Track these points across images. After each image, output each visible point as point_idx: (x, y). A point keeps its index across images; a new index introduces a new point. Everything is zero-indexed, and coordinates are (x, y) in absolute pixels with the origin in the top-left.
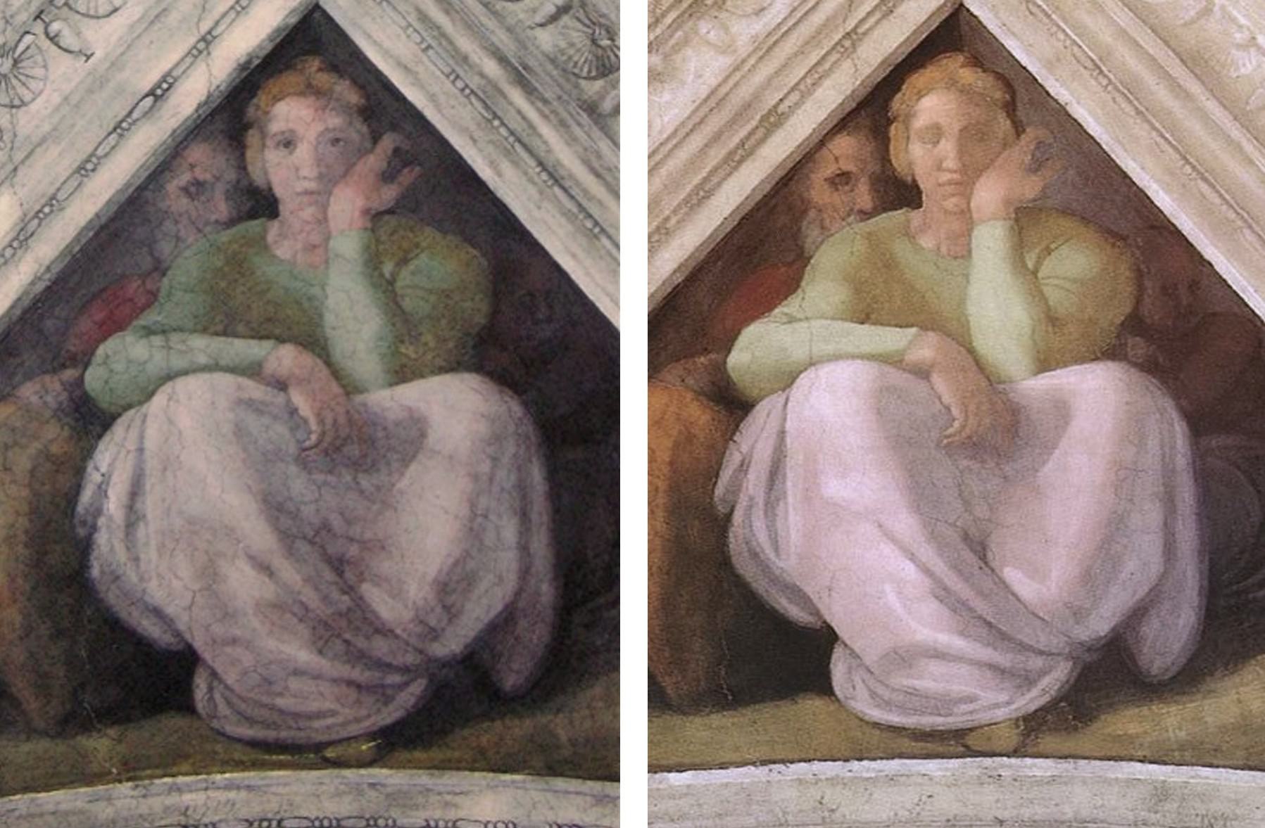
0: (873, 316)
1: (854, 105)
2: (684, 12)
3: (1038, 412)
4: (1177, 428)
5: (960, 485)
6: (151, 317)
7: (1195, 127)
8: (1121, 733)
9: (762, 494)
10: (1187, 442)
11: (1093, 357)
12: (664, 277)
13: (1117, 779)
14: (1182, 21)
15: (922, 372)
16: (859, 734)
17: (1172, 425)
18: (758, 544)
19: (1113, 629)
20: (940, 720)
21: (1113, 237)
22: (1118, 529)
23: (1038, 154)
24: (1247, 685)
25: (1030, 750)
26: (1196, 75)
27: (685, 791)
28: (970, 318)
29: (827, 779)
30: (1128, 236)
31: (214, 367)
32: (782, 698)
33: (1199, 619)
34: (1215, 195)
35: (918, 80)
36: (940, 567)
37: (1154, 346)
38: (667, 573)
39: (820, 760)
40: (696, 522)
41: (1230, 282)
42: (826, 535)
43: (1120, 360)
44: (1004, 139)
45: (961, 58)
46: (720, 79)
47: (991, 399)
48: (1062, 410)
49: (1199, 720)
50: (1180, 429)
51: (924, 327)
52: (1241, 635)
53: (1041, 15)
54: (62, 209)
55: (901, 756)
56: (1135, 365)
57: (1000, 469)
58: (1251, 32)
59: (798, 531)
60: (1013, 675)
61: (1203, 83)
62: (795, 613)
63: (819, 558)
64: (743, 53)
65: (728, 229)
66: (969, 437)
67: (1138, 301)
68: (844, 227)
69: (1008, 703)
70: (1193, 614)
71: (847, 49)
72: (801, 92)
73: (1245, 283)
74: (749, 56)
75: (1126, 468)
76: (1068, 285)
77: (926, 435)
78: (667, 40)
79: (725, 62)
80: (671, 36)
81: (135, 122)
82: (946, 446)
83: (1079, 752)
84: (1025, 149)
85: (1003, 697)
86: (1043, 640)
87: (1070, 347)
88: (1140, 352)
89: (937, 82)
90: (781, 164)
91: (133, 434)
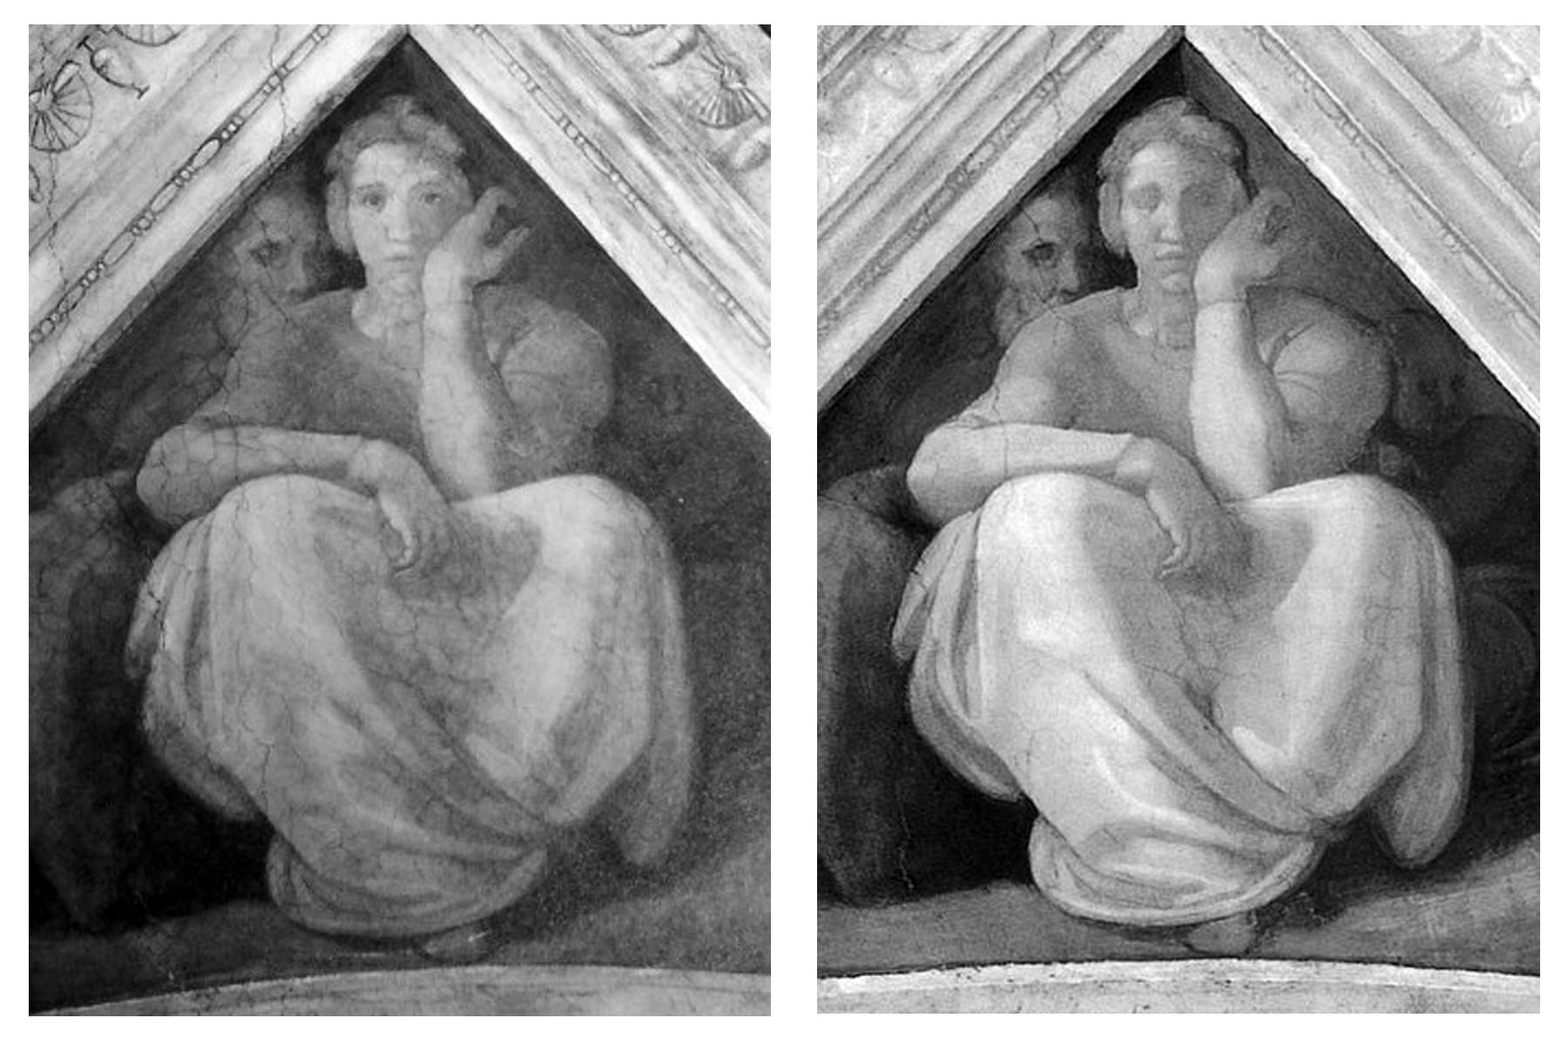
0: (1079, 420)
1: (1057, 161)
2: (856, 48)
3: (1274, 537)
4: (1438, 557)
5: (1181, 626)
6: (214, 408)
7: (1457, 187)
8: (1371, 929)
9: (949, 637)
10: (1449, 574)
11: (1338, 469)
12: (833, 372)
13: (1366, 986)
14: (1443, 59)
15: (1137, 488)
16: (1063, 931)
17: (1432, 553)
18: (944, 699)
19: (1363, 802)
20: (1158, 913)
21: (1362, 323)
22: (1367, 680)
23: (1274, 221)
24: (1520, 870)
25: (1265, 950)
26: (1460, 125)
27: (857, 1000)
28: (1193, 422)
29: (1025, 986)
30: (1379, 322)
31: (292, 468)
32: (971, 887)
33: (1463, 790)
34: (1482, 271)
35: (1132, 130)
36: (1157, 726)
37: (1411, 457)
38: (837, 734)
39: (1016, 963)
40: (871, 672)
41: (1499, 378)
42: (1024, 688)
43: (1370, 473)
44: (1233, 203)
45: (1183, 104)
46: (899, 130)
47: (1218, 522)
48: (1301, 534)
49: (1463, 913)
50: (1440, 557)
51: (1140, 434)
52: (1512, 810)
53: (1277, 52)
54: (109, 276)
55: (1112, 958)
56: (1388, 479)
57: (1230, 607)
58: (1525, 73)
59: (991, 682)
60: (1244, 859)
61: (1468, 134)
62: (987, 782)
63: (1015, 715)
64: (926, 97)
65: (909, 313)
66: (1193, 568)
67: (1392, 401)
68: (1045, 311)
69: (1238, 893)
70: (1456, 784)
71: (1048, 93)
72: (995, 145)
73: (1518, 380)
74: (933, 101)
75: (1378, 606)
76: (1308, 382)
77: (1142, 565)
78: (836, 82)
79: (902, 109)
80: (841, 77)
81: (197, 170)
82: (1165, 579)
83: (1322, 953)
84: (1258, 215)
85: (1233, 886)
86: (1280, 816)
87: (1312, 457)
88: (1394, 463)
89: (1154, 134)
90: (971, 233)
91: (195, 550)
